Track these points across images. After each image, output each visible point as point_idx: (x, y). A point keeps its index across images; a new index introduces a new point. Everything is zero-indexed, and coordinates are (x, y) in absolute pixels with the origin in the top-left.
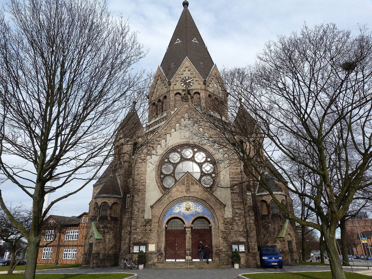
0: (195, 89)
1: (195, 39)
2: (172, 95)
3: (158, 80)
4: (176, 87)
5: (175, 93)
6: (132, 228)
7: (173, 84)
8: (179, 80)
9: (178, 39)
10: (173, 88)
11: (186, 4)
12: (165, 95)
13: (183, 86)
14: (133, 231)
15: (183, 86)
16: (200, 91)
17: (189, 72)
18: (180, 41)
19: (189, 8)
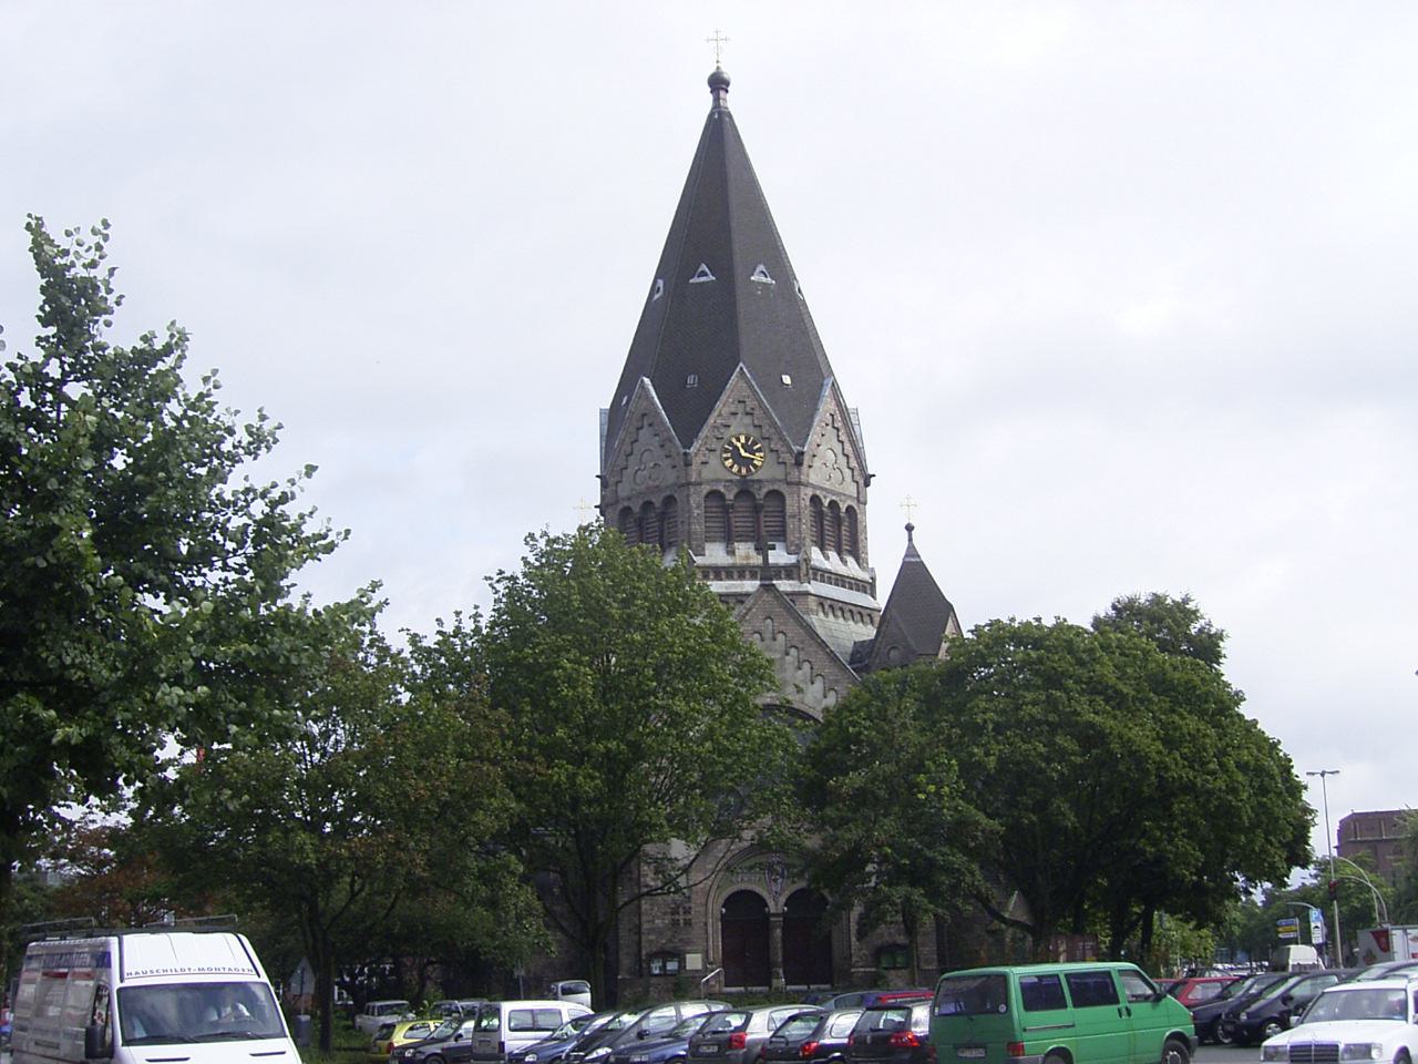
1: (761, 267)
2: (696, 499)
3: (642, 428)
4: (707, 473)
5: (705, 492)
6: (644, 918)
7: (696, 461)
9: (704, 267)
10: (699, 474)
11: (718, 84)
12: (668, 493)
13: (732, 467)
14: (645, 926)
15: (732, 467)
16: (783, 489)
17: (748, 420)
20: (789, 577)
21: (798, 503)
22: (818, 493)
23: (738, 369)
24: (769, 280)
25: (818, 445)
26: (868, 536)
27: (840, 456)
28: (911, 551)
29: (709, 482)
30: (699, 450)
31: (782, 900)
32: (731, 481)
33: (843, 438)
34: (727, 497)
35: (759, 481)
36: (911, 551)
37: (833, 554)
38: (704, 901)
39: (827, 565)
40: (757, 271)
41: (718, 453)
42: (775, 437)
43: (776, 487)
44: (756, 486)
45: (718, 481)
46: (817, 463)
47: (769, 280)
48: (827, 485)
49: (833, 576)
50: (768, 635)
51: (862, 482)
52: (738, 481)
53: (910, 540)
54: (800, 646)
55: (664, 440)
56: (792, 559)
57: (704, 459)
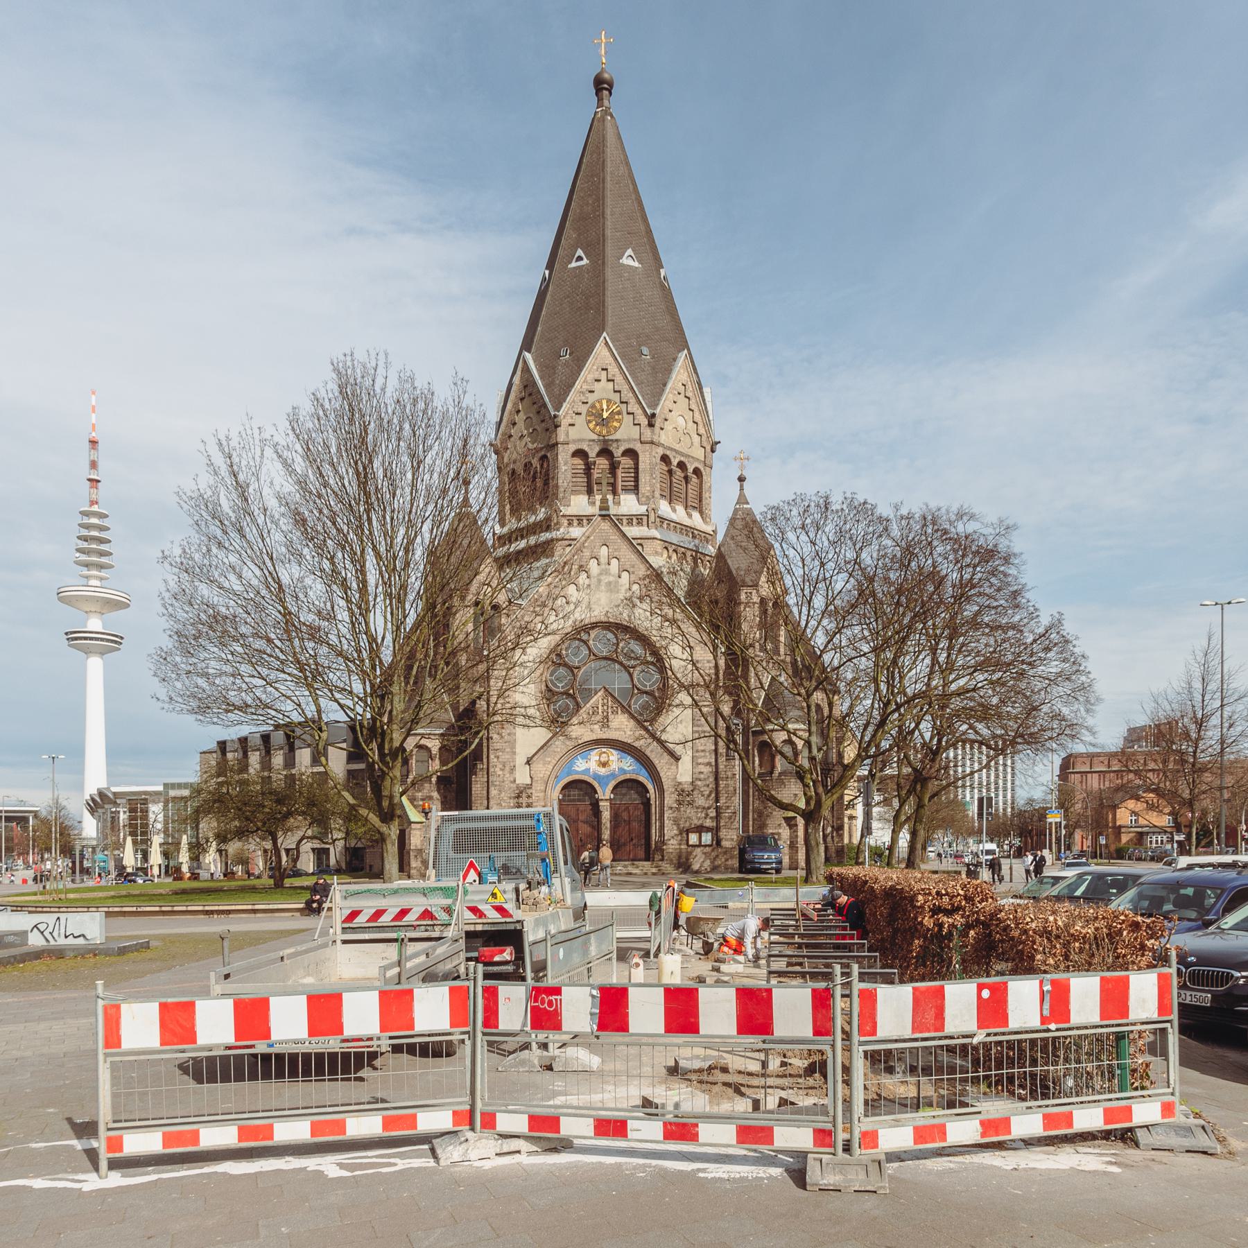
0: (624, 441)
1: (629, 252)
8: (584, 409)
9: (580, 252)
16: (638, 447)
18: (585, 261)
19: (615, 102)
20: (640, 523)
21: (648, 459)
22: (668, 453)
23: (602, 338)
24: (636, 264)
25: (670, 411)
26: (712, 495)
27: (691, 423)
28: (742, 499)
29: (574, 441)
30: (567, 413)
31: (611, 787)
32: (594, 440)
33: (693, 407)
34: (590, 455)
35: (617, 441)
36: (742, 499)
37: (680, 509)
38: (543, 788)
39: (674, 517)
40: (626, 254)
41: (584, 415)
42: (633, 401)
43: (631, 446)
44: (615, 445)
45: (583, 440)
46: (668, 426)
47: (636, 264)
48: (677, 447)
49: (678, 526)
50: (603, 560)
51: (708, 448)
52: (599, 440)
53: (742, 489)
54: (631, 570)
55: (540, 407)
56: (642, 509)
57: (571, 421)
